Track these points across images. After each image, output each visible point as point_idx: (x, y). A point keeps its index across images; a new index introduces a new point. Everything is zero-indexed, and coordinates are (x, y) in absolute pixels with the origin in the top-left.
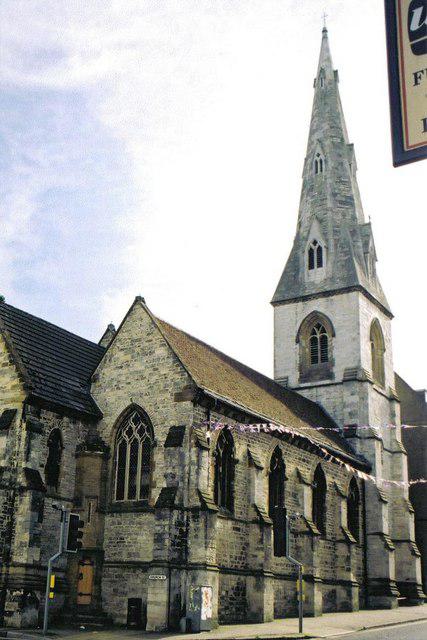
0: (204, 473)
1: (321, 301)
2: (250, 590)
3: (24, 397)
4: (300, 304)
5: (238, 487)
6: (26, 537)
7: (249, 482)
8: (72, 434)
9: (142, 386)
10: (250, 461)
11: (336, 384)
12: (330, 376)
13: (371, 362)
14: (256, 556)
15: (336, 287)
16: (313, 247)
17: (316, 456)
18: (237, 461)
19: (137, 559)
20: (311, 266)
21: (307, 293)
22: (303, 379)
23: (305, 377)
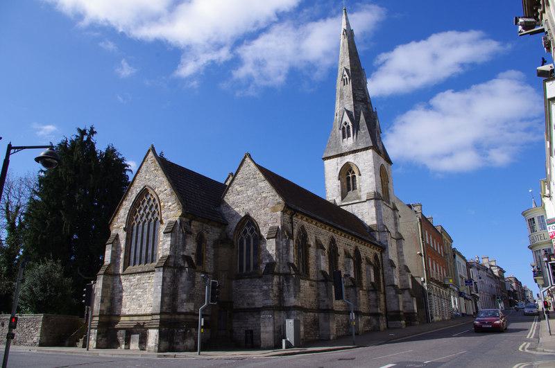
0: (292, 253)
2: (321, 321)
3: (180, 213)
5: (312, 261)
6: (184, 296)
7: (318, 258)
8: (212, 234)
9: (251, 205)
10: (319, 245)
12: (359, 198)
14: (324, 301)
15: (360, 148)
16: (345, 126)
18: (310, 246)
19: (253, 307)
20: (344, 137)
23: (343, 196)
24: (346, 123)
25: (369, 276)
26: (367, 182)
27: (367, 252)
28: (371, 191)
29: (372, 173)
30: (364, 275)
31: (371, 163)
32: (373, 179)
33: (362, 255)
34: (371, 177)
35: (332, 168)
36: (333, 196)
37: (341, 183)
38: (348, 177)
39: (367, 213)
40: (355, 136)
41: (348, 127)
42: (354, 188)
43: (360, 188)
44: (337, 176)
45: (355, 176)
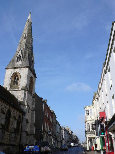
1: (19, 69)
4: (13, 69)
11: (19, 90)
12: (18, 88)
13: (29, 85)
15: (23, 66)
16: (19, 56)
17: (9, 107)
20: (17, 61)
21: (16, 67)
22: (10, 88)
23: (11, 87)
24: (19, 55)
25: (14, 124)
26: (23, 82)
27: (14, 113)
28: (24, 86)
29: (26, 78)
30: (11, 124)
31: (27, 74)
32: (26, 81)
33: (12, 114)
34: (25, 80)
35: (9, 73)
36: (6, 86)
37: (12, 80)
38: (15, 78)
39: (19, 95)
40: (22, 60)
41: (20, 57)
42: (17, 84)
43: (19, 84)
44: (10, 77)
45: (18, 79)
